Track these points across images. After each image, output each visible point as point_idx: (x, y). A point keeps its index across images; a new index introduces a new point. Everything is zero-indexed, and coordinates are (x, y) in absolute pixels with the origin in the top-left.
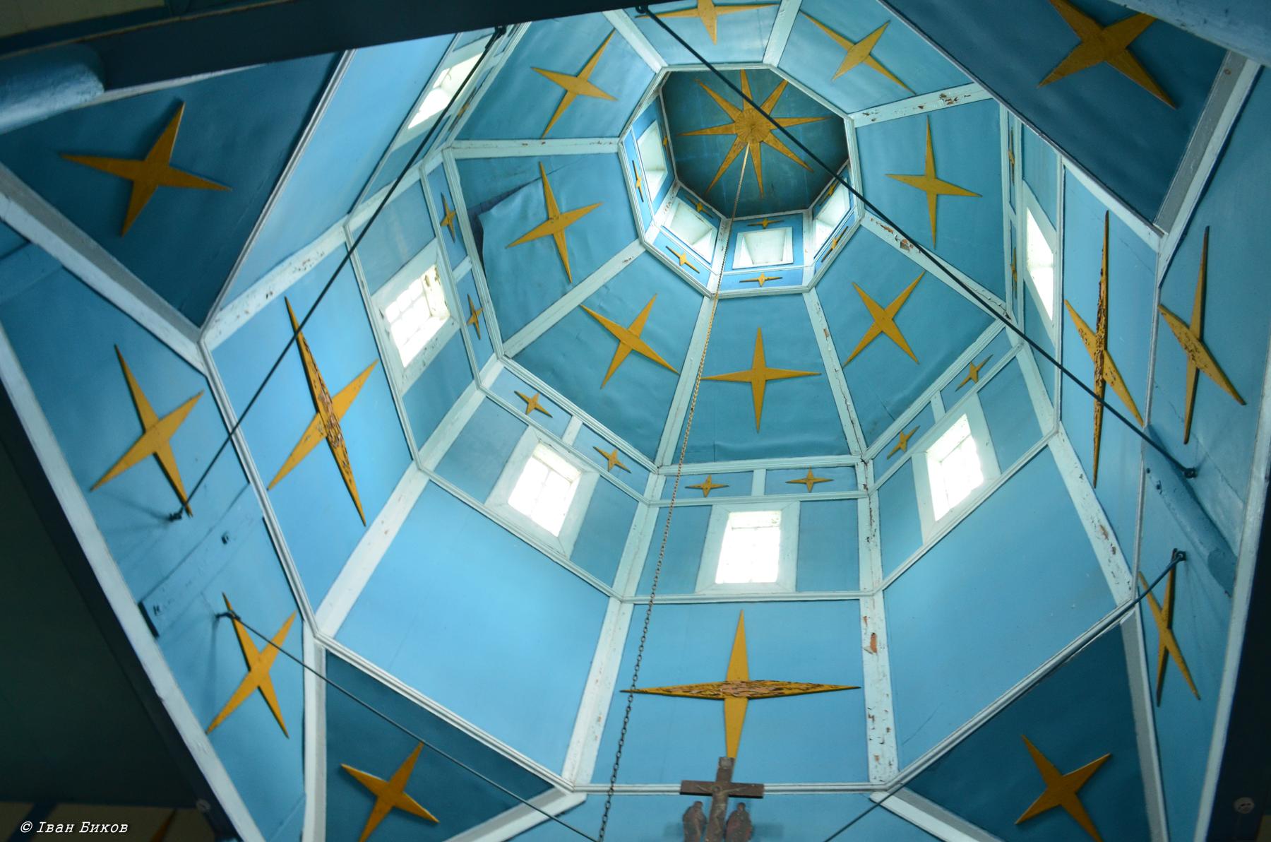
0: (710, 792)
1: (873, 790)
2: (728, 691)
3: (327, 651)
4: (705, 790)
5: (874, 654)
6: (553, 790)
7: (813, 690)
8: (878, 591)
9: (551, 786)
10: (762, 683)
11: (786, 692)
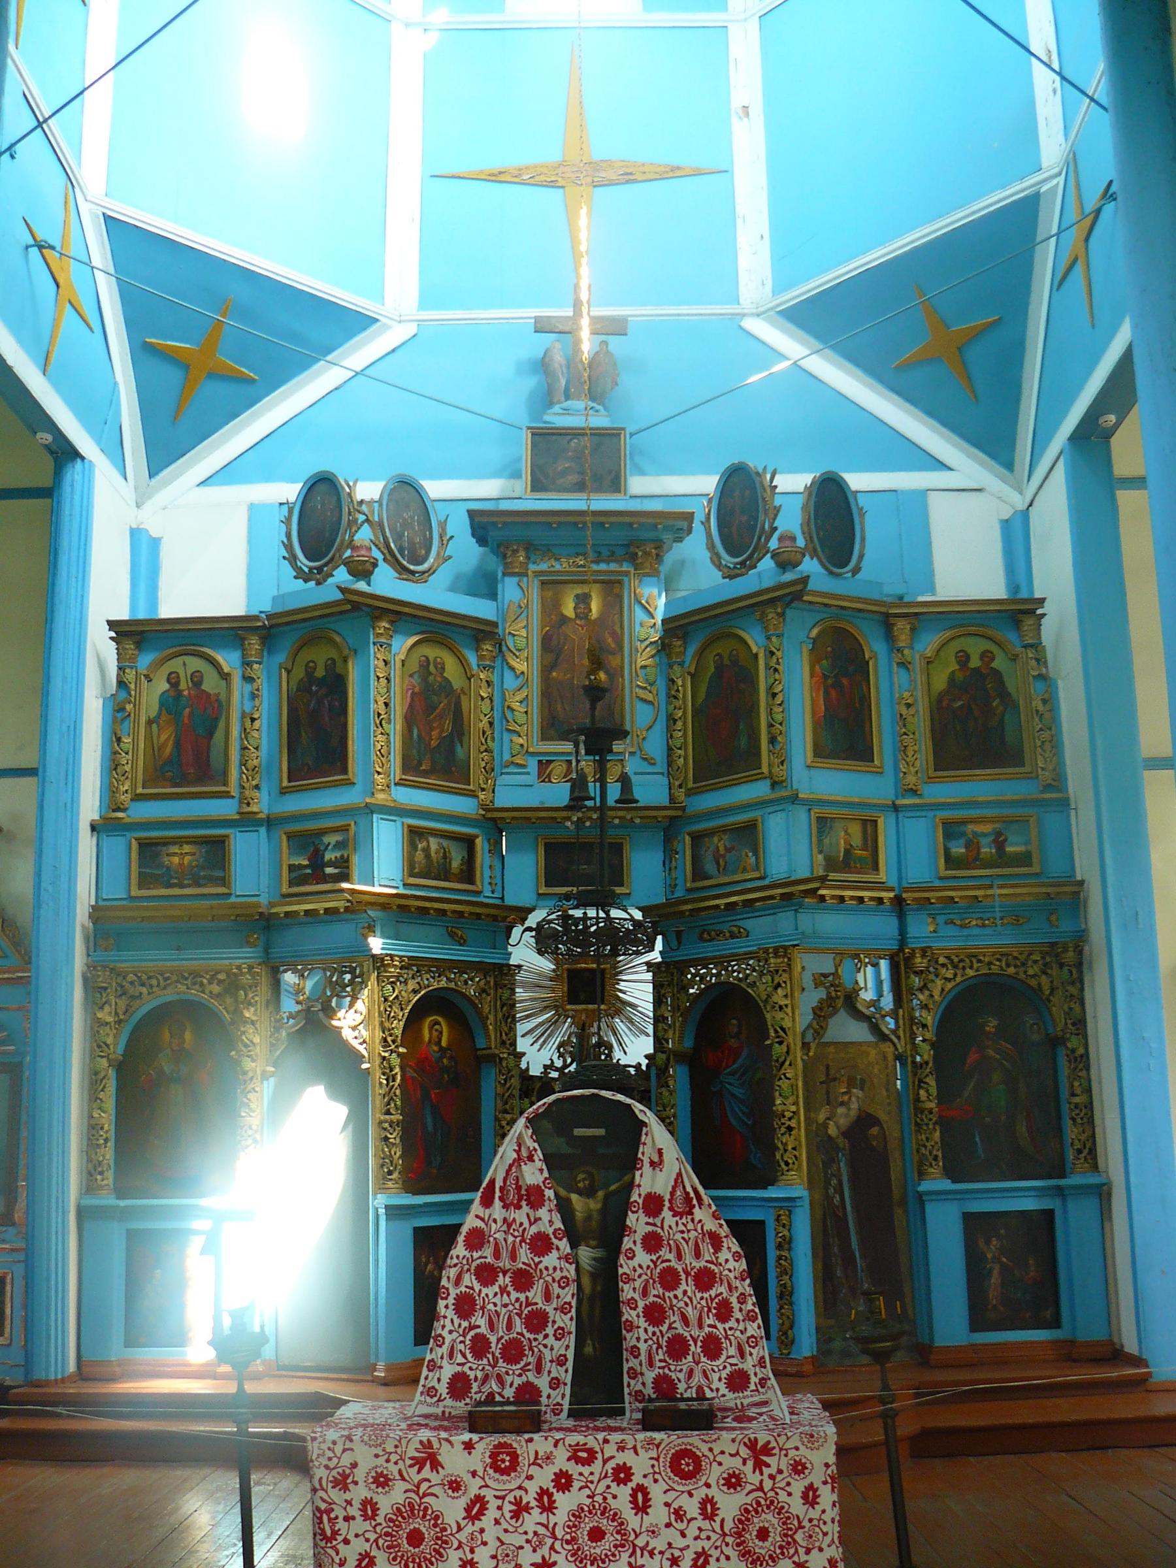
0: (567, 329)
1: (744, 315)
2: (567, 175)
3: (104, 214)
4: (561, 327)
5: (745, 120)
6: (378, 324)
7: (671, 175)
8: (753, 15)
9: (377, 320)
10: (609, 163)
11: (639, 177)
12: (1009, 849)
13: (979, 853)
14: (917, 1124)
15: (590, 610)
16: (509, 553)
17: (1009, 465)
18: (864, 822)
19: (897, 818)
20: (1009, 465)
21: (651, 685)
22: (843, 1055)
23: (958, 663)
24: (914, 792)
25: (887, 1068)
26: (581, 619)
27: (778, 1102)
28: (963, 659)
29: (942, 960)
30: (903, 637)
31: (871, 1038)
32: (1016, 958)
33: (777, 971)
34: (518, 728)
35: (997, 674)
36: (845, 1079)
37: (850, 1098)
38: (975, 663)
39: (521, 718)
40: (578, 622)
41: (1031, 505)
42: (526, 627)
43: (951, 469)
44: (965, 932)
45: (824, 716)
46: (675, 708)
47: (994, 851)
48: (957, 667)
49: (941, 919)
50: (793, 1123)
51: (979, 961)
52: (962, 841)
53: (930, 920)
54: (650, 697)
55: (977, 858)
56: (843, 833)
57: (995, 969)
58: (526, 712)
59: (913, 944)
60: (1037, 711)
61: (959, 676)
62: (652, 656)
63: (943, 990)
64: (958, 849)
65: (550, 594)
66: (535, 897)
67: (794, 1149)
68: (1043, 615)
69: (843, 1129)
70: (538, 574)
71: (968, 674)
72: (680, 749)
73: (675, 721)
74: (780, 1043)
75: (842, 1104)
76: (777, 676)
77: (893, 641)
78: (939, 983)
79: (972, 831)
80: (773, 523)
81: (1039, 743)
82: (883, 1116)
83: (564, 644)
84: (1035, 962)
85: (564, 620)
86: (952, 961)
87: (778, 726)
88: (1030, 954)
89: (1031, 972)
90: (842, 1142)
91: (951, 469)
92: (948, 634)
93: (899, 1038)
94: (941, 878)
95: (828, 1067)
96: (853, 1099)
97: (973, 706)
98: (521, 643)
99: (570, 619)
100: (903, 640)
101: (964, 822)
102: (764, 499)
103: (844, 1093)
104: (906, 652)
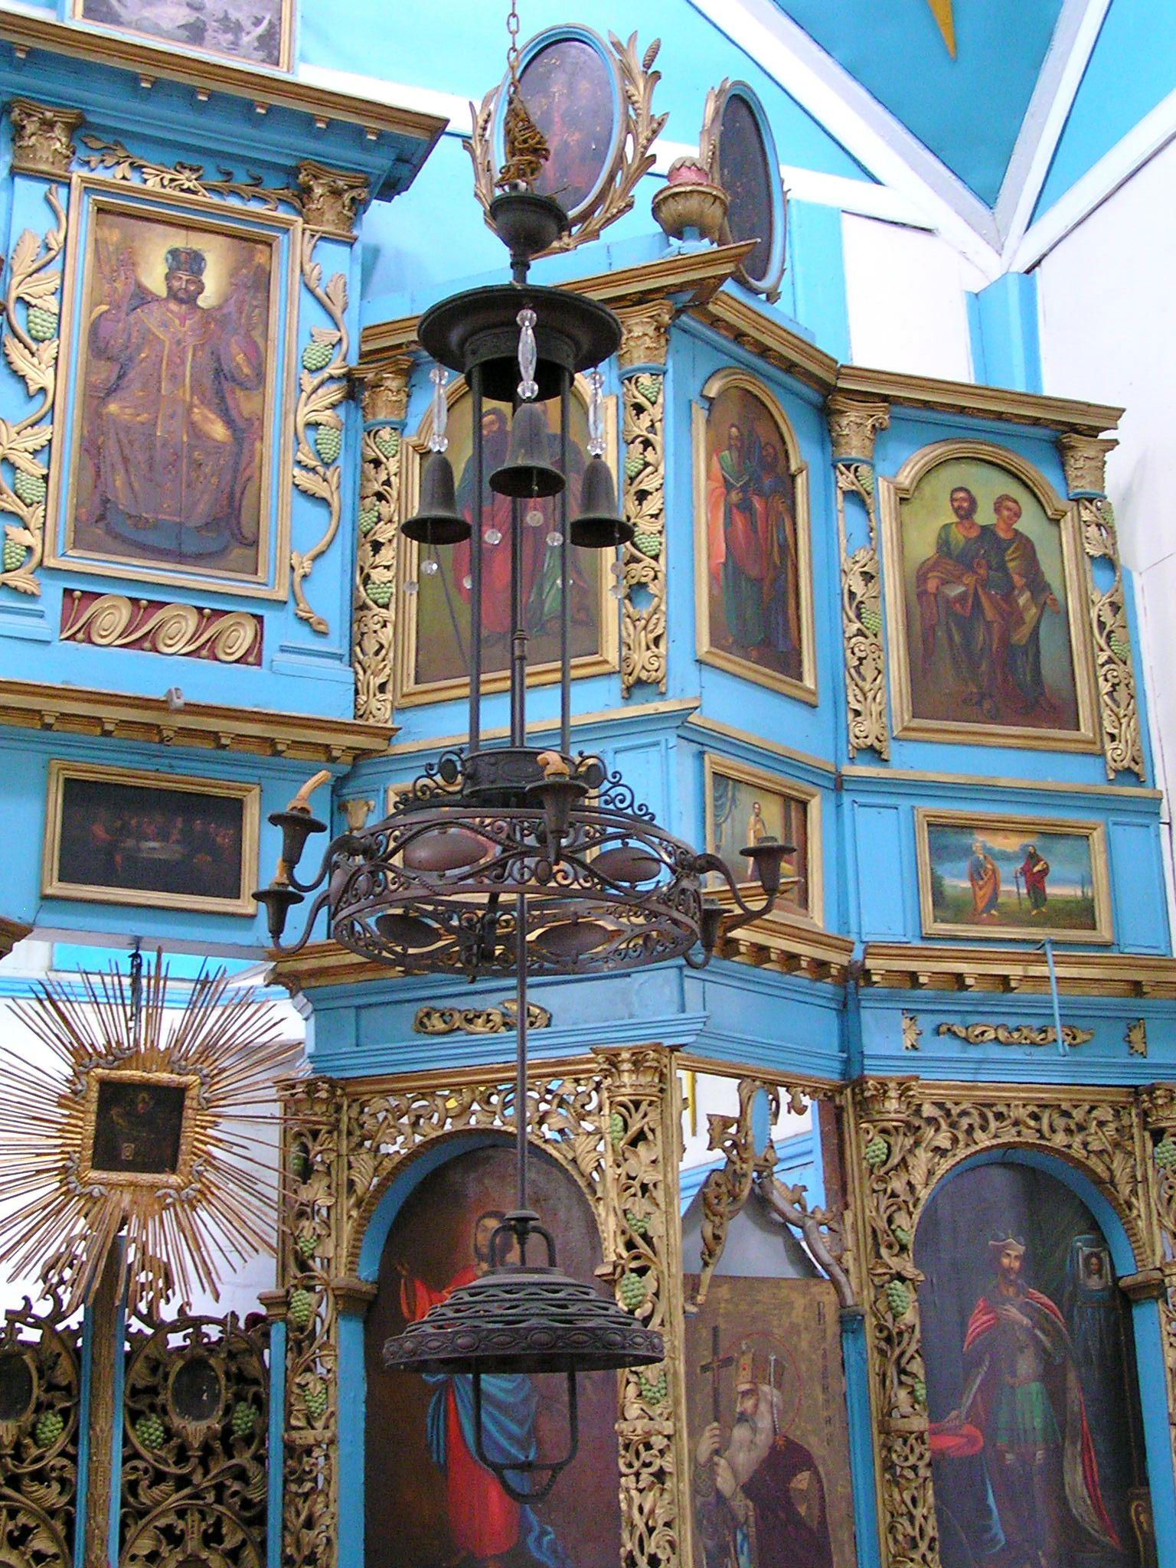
12: (1053, 890)
13: (995, 893)
14: (889, 1467)
15: (201, 289)
16: (30, 128)
17: (988, 197)
18: (787, 799)
19: (839, 806)
20: (988, 197)
21: (327, 465)
22: (743, 1307)
23: (957, 510)
24: (875, 754)
25: (824, 1338)
26: (181, 301)
27: (633, 1410)
28: (966, 507)
29: (928, 1110)
30: (855, 441)
31: (790, 1272)
32: (1066, 1114)
33: (637, 1104)
34: (24, 511)
35: (1026, 547)
36: (746, 1360)
37: (756, 1406)
38: (985, 516)
39: (33, 489)
40: (173, 306)
41: (1038, 263)
42: (60, 292)
43: (878, 182)
44: (974, 1053)
45: (725, 564)
46: (379, 519)
47: (1023, 891)
48: (954, 519)
49: (926, 1022)
50: (668, 1463)
51: (1000, 1116)
52: (964, 866)
53: (905, 1023)
54: (322, 490)
55: (993, 901)
56: (752, 818)
57: (1030, 1137)
58: (46, 478)
59: (873, 1072)
60: (1102, 625)
61: (958, 537)
62: (333, 406)
63: (930, 1173)
64: (958, 882)
65: (114, 236)
66: (34, 901)
67: (667, 1524)
68: (1115, 442)
69: (744, 1478)
70: (90, 188)
71: (974, 534)
72: (386, 606)
73: (377, 546)
74: (641, 1271)
75: (743, 1418)
76: (650, 456)
77: (835, 444)
78: (922, 1158)
79: (984, 847)
80: (646, 148)
81: (1105, 688)
82: (816, 1446)
83: (139, 350)
84: (1101, 1124)
85: (142, 297)
86: (948, 1113)
87: (648, 561)
88: (1092, 1108)
89: (1095, 1146)
90: (743, 1506)
91: (878, 182)
92: (940, 450)
93: (846, 1271)
94: (923, 938)
95: (715, 1329)
96: (763, 1407)
97: (983, 599)
98: (44, 324)
99: (157, 299)
100: (855, 445)
101: (967, 827)
102: (628, 98)
103: (745, 1394)
104: (864, 469)
